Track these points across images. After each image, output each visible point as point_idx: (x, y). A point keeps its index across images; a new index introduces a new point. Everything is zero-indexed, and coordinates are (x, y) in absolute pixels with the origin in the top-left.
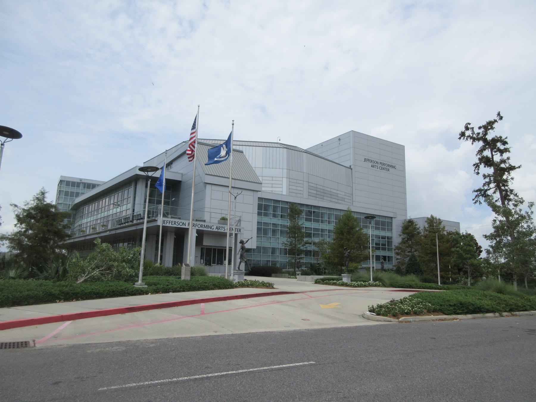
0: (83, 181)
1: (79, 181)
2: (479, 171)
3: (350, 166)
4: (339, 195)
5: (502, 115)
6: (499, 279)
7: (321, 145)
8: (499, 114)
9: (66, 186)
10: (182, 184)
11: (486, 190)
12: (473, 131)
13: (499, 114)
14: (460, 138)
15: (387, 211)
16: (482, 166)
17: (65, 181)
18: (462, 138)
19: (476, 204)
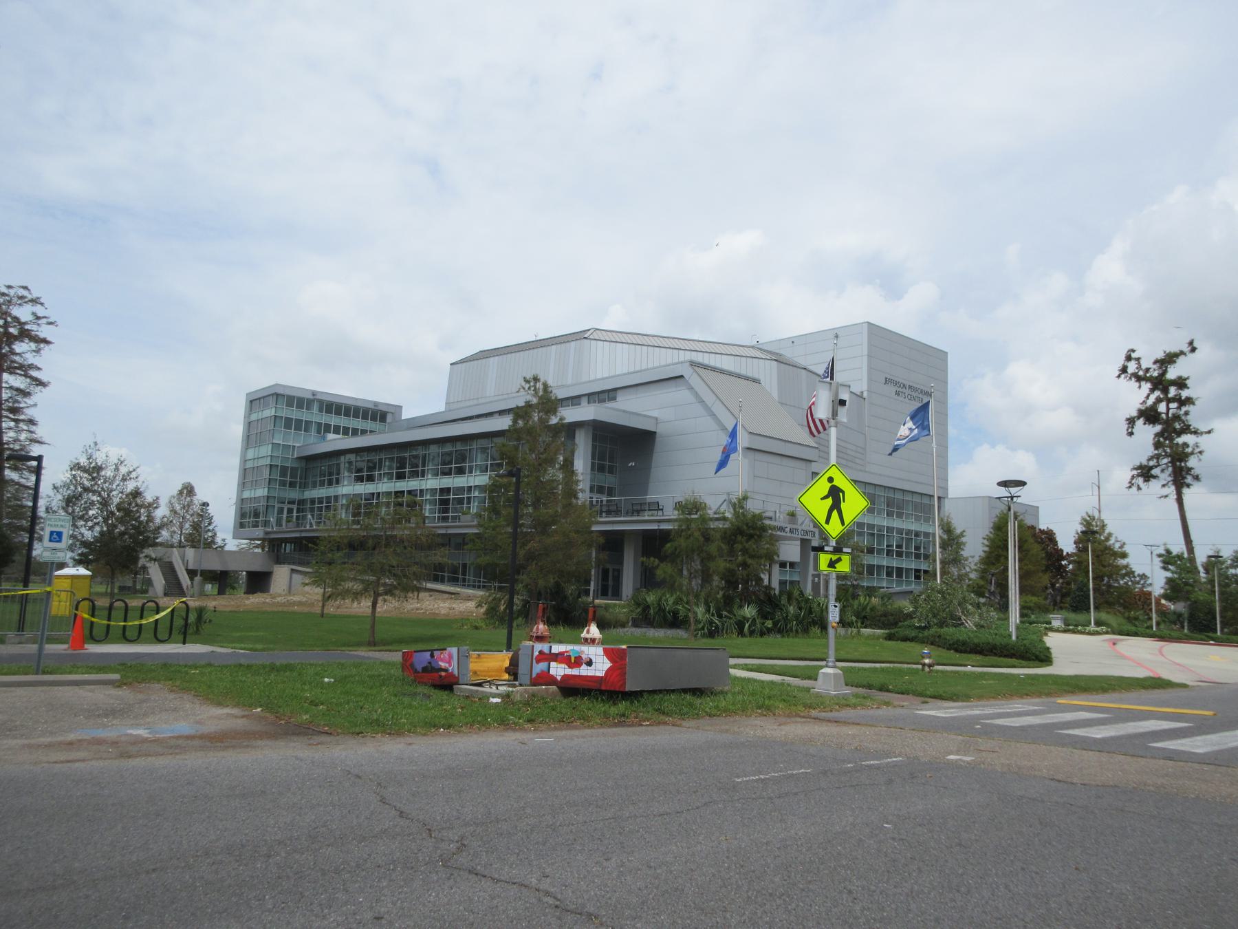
0: (319, 397)
1: (311, 397)
2: (1134, 430)
3: (862, 392)
4: (849, 452)
5: (1195, 344)
6: (1186, 627)
7: (795, 343)
8: (1191, 343)
9: (286, 406)
10: (658, 440)
11: (1151, 468)
12: (1139, 363)
13: (1191, 343)
14: (1119, 376)
15: (880, 475)
16: (1140, 422)
17: (283, 396)
18: (1123, 376)
19: (1130, 489)
